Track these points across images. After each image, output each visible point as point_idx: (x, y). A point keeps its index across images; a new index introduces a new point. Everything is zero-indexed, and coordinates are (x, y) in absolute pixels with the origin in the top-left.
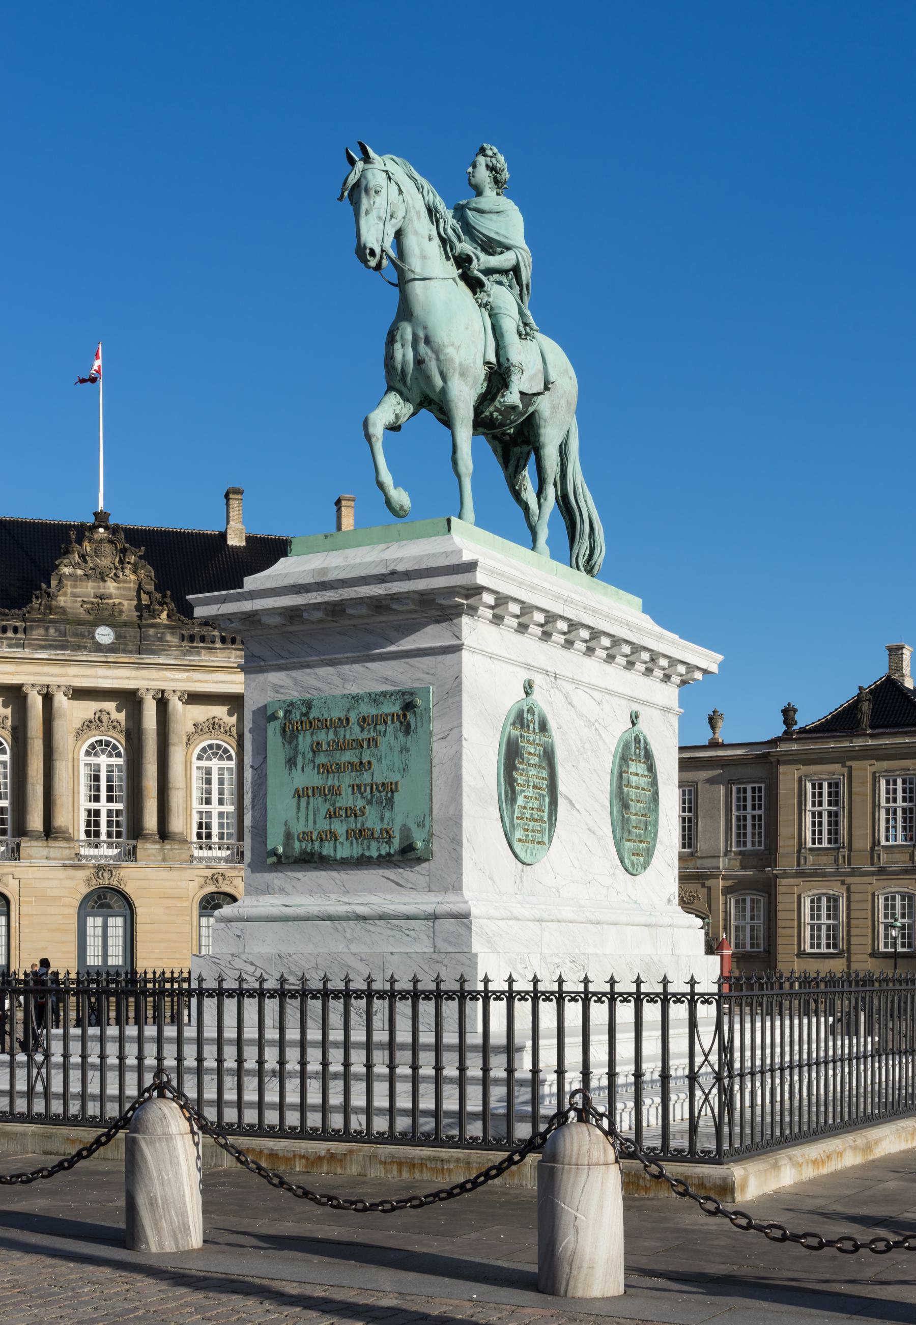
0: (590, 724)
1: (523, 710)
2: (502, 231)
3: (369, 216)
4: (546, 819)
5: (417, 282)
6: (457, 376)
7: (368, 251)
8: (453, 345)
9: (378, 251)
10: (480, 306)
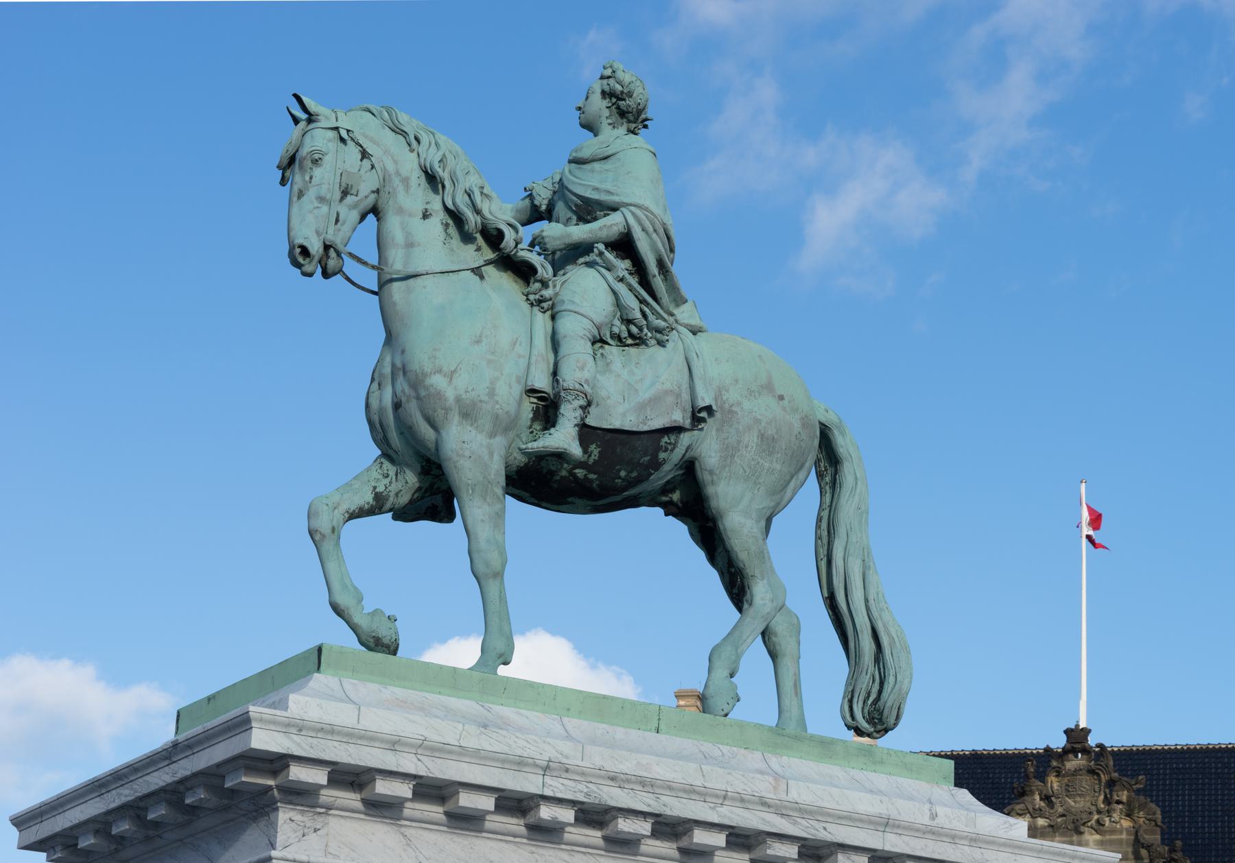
2: (608, 186)
3: (304, 199)
5: (396, 285)
6: (456, 419)
7: (298, 250)
8: (440, 371)
9: (315, 248)
10: (532, 305)
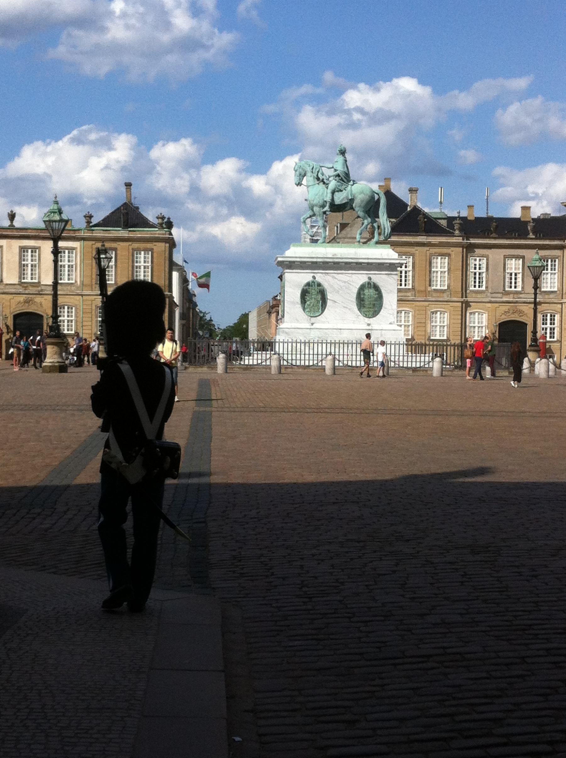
0: (345, 282)
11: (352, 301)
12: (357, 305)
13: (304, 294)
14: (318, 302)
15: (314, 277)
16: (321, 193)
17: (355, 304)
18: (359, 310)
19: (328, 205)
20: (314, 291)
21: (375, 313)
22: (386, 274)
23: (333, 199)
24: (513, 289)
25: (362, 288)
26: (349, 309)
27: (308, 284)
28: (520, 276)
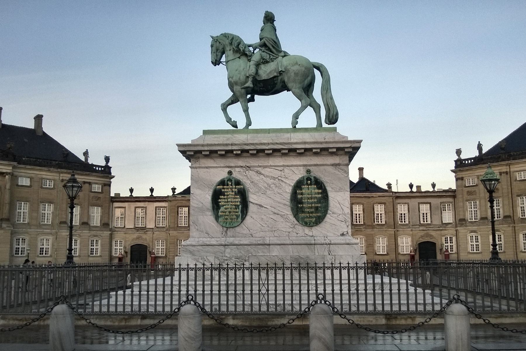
0: (274, 178)
1: (224, 181)
4: (240, 213)
11: (285, 205)
12: (292, 209)
13: (217, 195)
14: (237, 207)
15: (230, 173)
16: (242, 68)
17: (290, 208)
18: (295, 217)
19: (250, 79)
20: (230, 191)
21: (319, 220)
22: (333, 165)
23: (257, 73)
24: (425, 222)
25: (299, 185)
26: (282, 216)
27: (222, 183)
28: (429, 215)
